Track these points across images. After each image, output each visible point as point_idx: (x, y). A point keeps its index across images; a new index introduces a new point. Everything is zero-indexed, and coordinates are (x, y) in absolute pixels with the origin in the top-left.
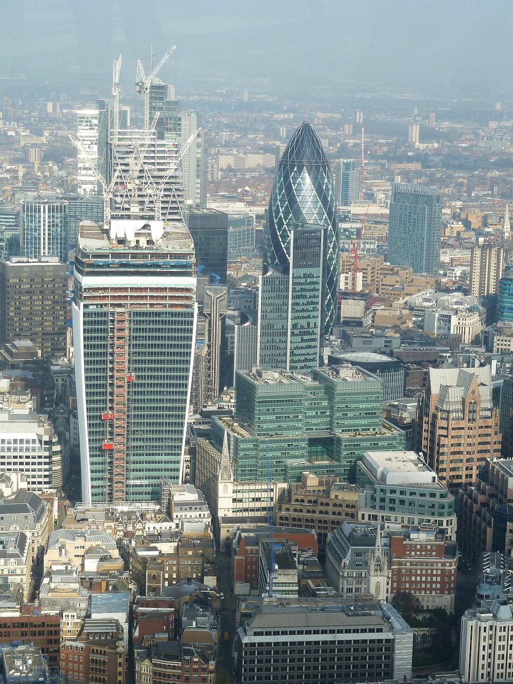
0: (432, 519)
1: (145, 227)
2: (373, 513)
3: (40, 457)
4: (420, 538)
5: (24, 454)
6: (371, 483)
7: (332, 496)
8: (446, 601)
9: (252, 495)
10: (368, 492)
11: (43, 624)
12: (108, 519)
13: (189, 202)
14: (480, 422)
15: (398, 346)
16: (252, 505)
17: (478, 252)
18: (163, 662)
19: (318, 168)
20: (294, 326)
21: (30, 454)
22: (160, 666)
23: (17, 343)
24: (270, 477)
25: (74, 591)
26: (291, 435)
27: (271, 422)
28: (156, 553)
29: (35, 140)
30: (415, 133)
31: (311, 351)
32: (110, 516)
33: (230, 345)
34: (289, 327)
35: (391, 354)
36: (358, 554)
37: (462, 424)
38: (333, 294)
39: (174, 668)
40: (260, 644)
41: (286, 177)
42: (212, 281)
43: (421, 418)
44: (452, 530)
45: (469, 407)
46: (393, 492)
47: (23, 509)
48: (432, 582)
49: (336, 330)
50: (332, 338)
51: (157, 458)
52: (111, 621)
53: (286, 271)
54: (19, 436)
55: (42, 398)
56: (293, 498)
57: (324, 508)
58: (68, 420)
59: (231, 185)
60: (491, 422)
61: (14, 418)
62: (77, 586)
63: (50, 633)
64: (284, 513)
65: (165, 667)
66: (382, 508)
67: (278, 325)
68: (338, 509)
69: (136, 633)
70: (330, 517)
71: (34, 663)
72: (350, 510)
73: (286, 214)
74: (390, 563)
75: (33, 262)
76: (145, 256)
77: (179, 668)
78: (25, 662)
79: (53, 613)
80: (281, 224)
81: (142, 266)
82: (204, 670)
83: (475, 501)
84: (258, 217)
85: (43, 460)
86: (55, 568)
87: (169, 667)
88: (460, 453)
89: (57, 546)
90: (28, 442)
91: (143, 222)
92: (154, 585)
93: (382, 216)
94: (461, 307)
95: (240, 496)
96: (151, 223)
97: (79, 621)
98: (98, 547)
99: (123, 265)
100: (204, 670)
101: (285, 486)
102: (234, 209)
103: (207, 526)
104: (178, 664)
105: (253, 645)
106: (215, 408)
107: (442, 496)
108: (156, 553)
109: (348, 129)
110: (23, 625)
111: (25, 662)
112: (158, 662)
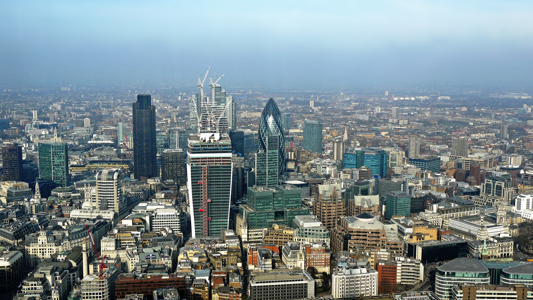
0: (321, 239)
1: (213, 135)
2: (299, 238)
4: (317, 246)
5: (171, 220)
6: (298, 227)
7: (284, 232)
8: (327, 270)
9: (255, 233)
10: (297, 230)
11: (178, 281)
12: (201, 243)
13: (230, 128)
14: (337, 204)
15: (307, 178)
16: (255, 237)
17: (336, 144)
19: (276, 114)
20: (269, 172)
21: (173, 220)
22: (221, 296)
23: (168, 181)
24: (261, 226)
25: (189, 269)
26: (268, 210)
27: (261, 206)
29: (175, 110)
30: (312, 104)
31: (275, 180)
32: (202, 242)
34: (267, 172)
35: (305, 181)
36: (294, 253)
37: (331, 205)
38: (283, 160)
39: (227, 296)
40: (258, 287)
41: (265, 118)
43: (316, 203)
44: (328, 244)
45: (334, 197)
46: (306, 230)
47: (170, 240)
48: (321, 263)
49: (284, 173)
50: (283, 176)
51: (219, 220)
52: (203, 280)
53: (265, 151)
54: (168, 214)
56: (270, 233)
57: (281, 237)
59: (247, 123)
60: (341, 204)
61: (166, 207)
62: (190, 267)
64: (266, 239)
65: (223, 296)
66: (302, 236)
67: (263, 171)
68: (286, 237)
69: (212, 284)
70: (283, 240)
72: (290, 237)
73: (265, 131)
74: (305, 256)
75: (173, 151)
76: (213, 146)
78: (171, 294)
79: (181, 277)
80: (263, 135)
81: (212, 149)
82: (237, 297)
83: (337, 233)
84: (256, 134)
86: (182, 261)
88: (330, 215)
90: (172, 216)
91: (212, 134)
92: (219, 266)
93: (301, 133)
94: (330, 164)
96: (215, 134)
98: (198, 253)
99: (205, 149)
100: (237, 297)
101: (267, 229)
102: (247, 131)
104: (228, 295)
107: (324, 231)
109: (288, 103)
110: (170, 281)
111: (171, 294)
112: (221, 294)
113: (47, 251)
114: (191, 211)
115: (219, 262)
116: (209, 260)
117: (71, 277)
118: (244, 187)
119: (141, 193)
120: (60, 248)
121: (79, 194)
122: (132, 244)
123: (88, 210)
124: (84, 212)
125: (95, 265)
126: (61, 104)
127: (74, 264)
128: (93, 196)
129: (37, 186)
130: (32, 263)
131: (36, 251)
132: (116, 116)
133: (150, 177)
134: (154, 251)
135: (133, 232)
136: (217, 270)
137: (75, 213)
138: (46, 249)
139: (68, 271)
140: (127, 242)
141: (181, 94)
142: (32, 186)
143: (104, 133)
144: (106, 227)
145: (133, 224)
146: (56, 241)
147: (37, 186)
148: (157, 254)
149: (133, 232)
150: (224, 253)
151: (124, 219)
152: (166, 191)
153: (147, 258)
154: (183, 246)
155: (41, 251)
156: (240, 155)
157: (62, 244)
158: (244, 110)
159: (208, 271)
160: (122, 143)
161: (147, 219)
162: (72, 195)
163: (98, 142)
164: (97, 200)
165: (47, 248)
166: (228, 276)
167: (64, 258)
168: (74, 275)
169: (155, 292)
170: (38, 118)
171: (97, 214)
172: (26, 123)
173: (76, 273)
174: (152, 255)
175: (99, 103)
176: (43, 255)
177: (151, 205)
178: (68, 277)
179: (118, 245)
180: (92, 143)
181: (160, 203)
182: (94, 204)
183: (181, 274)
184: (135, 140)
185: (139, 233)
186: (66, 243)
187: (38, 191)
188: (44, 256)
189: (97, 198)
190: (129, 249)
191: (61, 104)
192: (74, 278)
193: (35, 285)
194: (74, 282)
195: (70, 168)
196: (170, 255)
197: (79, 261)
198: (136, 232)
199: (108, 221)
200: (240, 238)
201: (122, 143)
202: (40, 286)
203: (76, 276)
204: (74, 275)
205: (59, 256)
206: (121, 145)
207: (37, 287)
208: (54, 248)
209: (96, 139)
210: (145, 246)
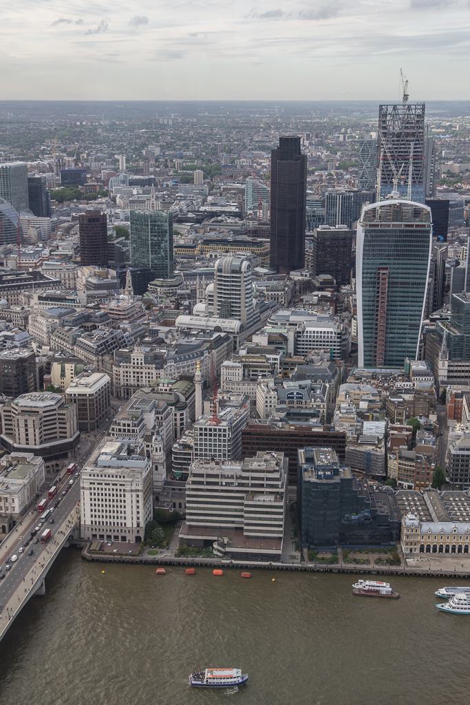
3: (335, 342)
18: (404, 463)
22: (403, 464)
25: (354, 418)
28: (402, 400)
33: (447, 279)
39: (411, 466)
42: (438, 240)
55: (336, 307)
58: (350, 321)
61: (320, 319)
63: (340, 442)
69: (389, 445)
71: (332, 457)
77: (413, 466)
78: (326, 458)
82: (428, 468)
85: (336, 344)
87: (408, 466)
89: (344, 393)
92: (400, 418)
95: (451, 368)
97: (356, 436)
100: (428, 468)
102: (455, 197)
103: (432, 386)
105: (458, 456)
106: (438, 317)
108: (402, 400)
110: (324, 436)
112: (402, 462)
113: (144, 375)
114: (358, 327)
115: (400, 411)
116: (383, 408)
117: (178, 417)
118: (445, 289)
119: (280, 293)
120: (162, 372)
121: (188, 291)
122: (267, 373)
123: (200, 317)
124: (196, 320)
125: (212, 401)
126: (161, 146)
127: (182, 398)
128: (210, 296)
129: (129, 278)
130: (122, 392)
131: (128, 374)
132: (242, 167)
133: (294, 269)
134: (300, 387)
135: (268, 356)
136: (397, 425)
137: (183, 320)
138: (142, 373)
139: (173, 408)
140: (259, 369)
141: (343, 130)
142: (122, 277)
143: (224, 194)
144: (228, 345)
145: (270, 343)
146: (157, 361)
147: (129, 278)
148: (304, 392)
149: (268, 356)
150: (407, 397)
151: (254, 333)
152: (320, 293)
153: (288, 398)
154: (343, 380)
155: (136, 375)
156: (442, 238)
157: (165, 367)
158: (447, 159)
159: (382, 424)
160: (251, 212)
161: (291, 336)
162: (179, 292)
163: (215, 209)
164: (215, 303)
165: (144, 371)
166: (414, 434)
167: (168, 389)
168: (182, 415)
169: (301, 451)
170: (127, 168)
171: (215, 325)
172: (110, 175)
173: (184, 412)
174: (298, 394)
175: (215, 145)
176: (138, 381)
177: (294, 313)
178: (174, 417)
179: (246, 374)
180: (205, 211)
181: (310, 312)
182: (212, 309)
183: (342, 425)
184: (273, 208)
185: (278, 357)
186: (171, 366)
187: (131, 284)
188: (140, 383)
189: (215, 299)
190: (262, 380)
191: (161, 146)
192: (182, 419)
193: (129, 425)
194: (182, 424)
195: (175, 249)
196: (324, 393)
197: (190, 393)
198: (275, 356)
199: (231, 336)
200: (436, 377)
201: (251, 212)
202: (135, 428)
203: (184, 417)
204: (182, 415)
205: (161, 385)
206: (250, 214)
207: (131, 428)
208: (154, 372)
209: (213, 204)
210: (286, 376)
